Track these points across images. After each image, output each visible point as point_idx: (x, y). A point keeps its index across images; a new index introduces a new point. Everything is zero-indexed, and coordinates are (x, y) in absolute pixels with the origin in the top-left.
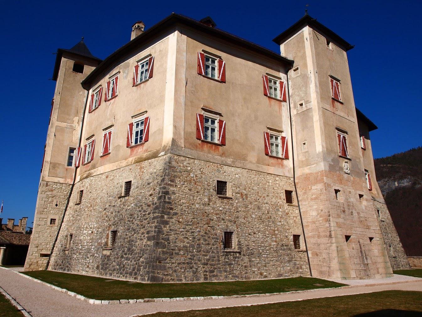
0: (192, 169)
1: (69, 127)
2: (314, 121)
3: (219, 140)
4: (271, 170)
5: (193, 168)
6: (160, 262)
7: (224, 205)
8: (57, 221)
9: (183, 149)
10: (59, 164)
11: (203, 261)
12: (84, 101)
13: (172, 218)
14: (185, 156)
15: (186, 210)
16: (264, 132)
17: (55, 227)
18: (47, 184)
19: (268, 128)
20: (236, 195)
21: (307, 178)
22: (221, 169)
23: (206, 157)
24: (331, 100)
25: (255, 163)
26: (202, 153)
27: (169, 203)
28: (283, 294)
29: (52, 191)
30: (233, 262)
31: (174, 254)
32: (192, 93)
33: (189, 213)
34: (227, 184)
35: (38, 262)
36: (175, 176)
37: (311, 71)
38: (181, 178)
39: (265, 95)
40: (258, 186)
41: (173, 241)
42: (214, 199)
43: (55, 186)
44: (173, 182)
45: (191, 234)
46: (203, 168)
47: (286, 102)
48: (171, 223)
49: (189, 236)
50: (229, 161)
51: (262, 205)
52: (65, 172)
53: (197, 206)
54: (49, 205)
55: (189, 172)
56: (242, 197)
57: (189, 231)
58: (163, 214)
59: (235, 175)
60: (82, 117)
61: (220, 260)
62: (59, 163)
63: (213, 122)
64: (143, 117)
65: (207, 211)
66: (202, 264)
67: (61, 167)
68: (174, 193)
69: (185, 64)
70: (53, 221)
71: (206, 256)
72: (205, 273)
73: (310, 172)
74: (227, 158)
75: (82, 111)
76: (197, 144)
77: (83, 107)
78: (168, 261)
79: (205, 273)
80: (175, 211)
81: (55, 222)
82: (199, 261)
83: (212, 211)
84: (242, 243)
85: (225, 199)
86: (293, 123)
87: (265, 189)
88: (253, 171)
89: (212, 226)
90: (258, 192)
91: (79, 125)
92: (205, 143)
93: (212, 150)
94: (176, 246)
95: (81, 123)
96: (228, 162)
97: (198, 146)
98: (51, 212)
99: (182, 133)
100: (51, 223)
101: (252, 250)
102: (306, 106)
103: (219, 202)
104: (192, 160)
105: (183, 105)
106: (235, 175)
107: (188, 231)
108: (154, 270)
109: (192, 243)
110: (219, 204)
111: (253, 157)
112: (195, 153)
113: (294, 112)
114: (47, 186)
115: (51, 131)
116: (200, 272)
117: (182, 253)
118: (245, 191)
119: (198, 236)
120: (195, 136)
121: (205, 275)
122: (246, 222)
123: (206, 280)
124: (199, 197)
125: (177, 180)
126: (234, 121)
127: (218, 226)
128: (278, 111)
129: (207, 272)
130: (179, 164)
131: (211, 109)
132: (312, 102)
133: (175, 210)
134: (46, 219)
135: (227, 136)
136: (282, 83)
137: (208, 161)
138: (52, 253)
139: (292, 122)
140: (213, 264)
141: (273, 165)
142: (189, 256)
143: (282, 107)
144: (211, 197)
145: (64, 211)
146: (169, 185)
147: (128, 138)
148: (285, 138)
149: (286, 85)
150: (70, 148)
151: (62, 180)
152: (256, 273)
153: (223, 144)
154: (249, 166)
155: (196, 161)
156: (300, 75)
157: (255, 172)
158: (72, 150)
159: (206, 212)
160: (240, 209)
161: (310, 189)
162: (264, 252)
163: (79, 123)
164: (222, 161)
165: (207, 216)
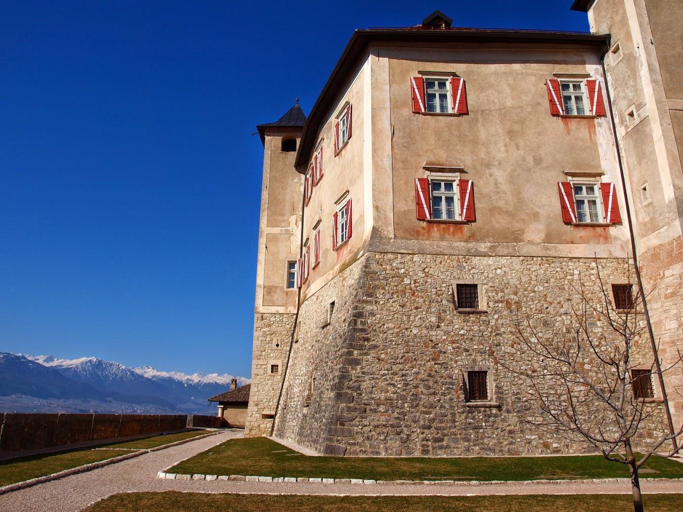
0: (407, 272)
1: (283, 232)
2: (655, 141)
3: (461, 215)
4: (580, 250)
5: (411, 269)
6: (342, 424)
7: (468, 326)
8: (280, 368)
9: (392, 241)
10: (276, 287)
11: (422, 422)
12: (301, 191)
13: (367, 354)
14: (395, 252)
15: (393, 339)
16: (558, 183)
17: (279, 377)
18: (262, 317)
19: (567, 174)
20: (496, 305)
21: (655, 254)
22: (465, 264)
23: (435, 247)
25: (540, 243)
26: (427, 242)
27: (363, 330)
28: (514, 484)
29: (270, 326)
30: (484, 424)
31: (368, 411)
32: (404, 147)
33: (398, 345)
34: (479, 287)
35: (259, 426)
36: (376, 287)
37: (638, 43)
38: (387, 288)
39: (554, 115)
40: (546, 285)
41: (368, 391)
42: (448, 316)
43: (273, 319)
44: (371, 297)
45: (401, 379)
46: (431, 267)
47: (605, 116)
48: (364, 363)
49: (397, 381)
50: (483, 247)
51: (553, 319)
52: (285, 298)
53: (415, 331)
54: (267, 345)
55: (401, 278)
56: (510, 308)
57: (396, 374)
58: (352, 350)
59: (496, 269)
60: (301, 213)
61: (457, 420)
62: (276, 285)
63: (449, 186)
64: (344, 203)
65: (434, 338)
66: (420, 428)
67: (278, 291)
68: (372, 314)
69: (388, 105)
70: (274, 368)
71: (430, 413)
72: (424, 443)
73: (660, 243)
74: (478, 244)
75: (300, 206)
76: (419, 229)
77: (300, 200)
78: (356, 422)
79: (424, 443)
80: (373, 343)
81: (277, 369)
82: (415, 422)
83: (444, 337)
84: (506, 390)
85: (471, 315)
86: (623, 154)
87: (562, 288)
88: (535, 259)
89: (443, 363)
90: (546, 295)
91: (297, 227)
92: (435, 225)
93: (449, 235)
94: (372, 399)
95: (300, 223)
96: (479, 249)
97: (422, 231)
98: (272, 355)
99: (391, 215)
100: (272, 372)
101: (526, 401)
102: (639, 115)
103: (458, 322)
104: (408, 257)
105: (389, 170)
106: (494, 271)
107: (395, 374)
108: (332, 437)
109: (402, 393)
110: (458, 324)
111: (535, 233)
112: (414, 243)
113: (621, 132)
114: (262, 320)
115: (262, 241)
116: (414, 440)
117: (382, 408)
118: (515, 297)
119: (415, 380)
120: (414, 217)
121: (423, 446)
122: (515, 352)
123: (425, 454)
124: (419, 316)
125: (379, 293)
126: (491, 175)
127: (456, 362)
128: (588, 136)
129: (427, 440)
130: (384, 267)
131: (442, 165)
132: (648, 105)
133: (374, 340)
134: (265, 366)
135: (478, 205)
136: (591, 85)
137: (439, 253)
138: (276, 414)
139: (620, 151)
140: (441, 427)
142: (396, 415)
143: (596, 127)
144: (443, 315)
145: (288, 353)
146: (367, 302)
147: (333, 236)
148: (609, 184)
149: (603, 85)
150: (288, 261)
151: (281, 310)
152: (534, 443)
153: (471, 218)
154: (526, 249)
155: (416, 258)
156: (623, 58)
157: (540, 258)
158: (292, 265)
159: (432, 341)
160: (502, 330)
161: (662, 277)
162: (554, 404)
163: (297, 223)
164: (469, 250)
165: (434, 347)
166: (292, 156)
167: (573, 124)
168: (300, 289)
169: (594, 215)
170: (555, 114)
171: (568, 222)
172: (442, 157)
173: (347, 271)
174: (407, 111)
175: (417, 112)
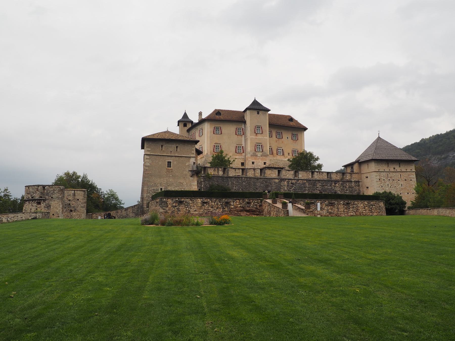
39: (236, 134)
47: (244, 135)
64: (201, 146)
69: (209, 132)
136: (243, 129)
141: (238, 155)
149: (244, 130)
166: (186, 128)
167: (239, 136)
169: (240, 151)
170: (236, 134)
173: (202, 159)
175: (214, 133)
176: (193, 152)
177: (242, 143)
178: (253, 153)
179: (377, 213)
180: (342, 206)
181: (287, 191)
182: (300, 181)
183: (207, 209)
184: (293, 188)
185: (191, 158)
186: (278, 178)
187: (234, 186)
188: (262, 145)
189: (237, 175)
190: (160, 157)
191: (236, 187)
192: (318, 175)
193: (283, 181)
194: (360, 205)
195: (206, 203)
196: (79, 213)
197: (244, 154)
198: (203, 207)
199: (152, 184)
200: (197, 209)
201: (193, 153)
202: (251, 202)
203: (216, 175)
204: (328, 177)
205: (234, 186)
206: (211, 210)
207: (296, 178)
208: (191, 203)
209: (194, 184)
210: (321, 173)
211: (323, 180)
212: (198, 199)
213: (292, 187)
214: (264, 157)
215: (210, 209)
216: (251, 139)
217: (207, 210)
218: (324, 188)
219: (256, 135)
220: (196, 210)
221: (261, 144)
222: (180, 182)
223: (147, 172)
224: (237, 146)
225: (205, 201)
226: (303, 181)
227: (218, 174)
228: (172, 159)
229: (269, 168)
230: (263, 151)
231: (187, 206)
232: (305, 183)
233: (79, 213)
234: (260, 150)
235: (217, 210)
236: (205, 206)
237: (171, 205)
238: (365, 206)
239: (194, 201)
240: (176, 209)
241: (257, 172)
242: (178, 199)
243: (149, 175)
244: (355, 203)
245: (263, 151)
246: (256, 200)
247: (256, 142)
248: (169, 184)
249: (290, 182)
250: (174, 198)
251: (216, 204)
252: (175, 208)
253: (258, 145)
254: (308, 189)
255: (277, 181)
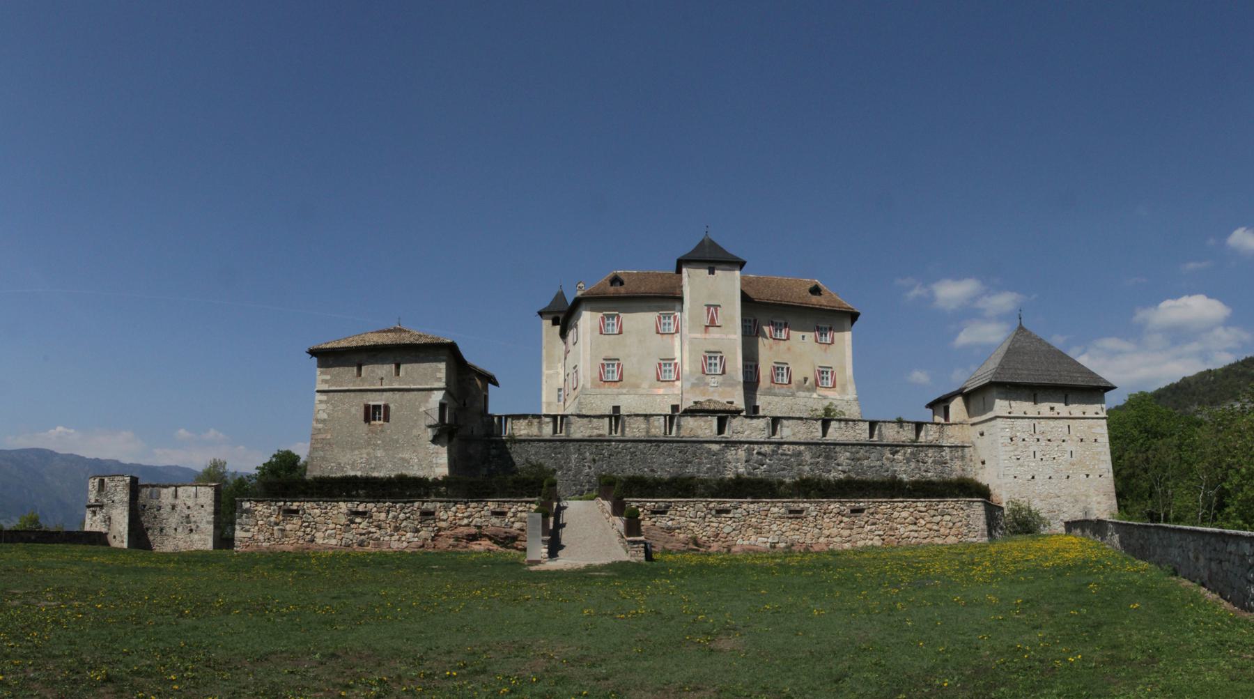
4: (661, 391)
24: (704, 327)
36: (583, 408)
50: (624, 391)
55: (592, 404)
99: (589, 379)
112: (598, 391)
120: (598, 379)
141: (664, 387)
153: (621, 380)
154: (641, 391)
155: (598, 396)
166: (558, 328)
168: (564, 403)
170: (658, 333)
171: (658, 380)
172: (611, 355)
174: (598, 332)
176: (439, 375)
177: (674, 355)
178: (698, 379)
179: (960, 536)
180: (834, 519)
181: (746, 475)
182: (785, 446)
183: (364, 531)
184: (765, 466)
185: (435, 392)
186: (717, 439)
187: (586, 464)
188: (721, 358)
189: (594, 434)
190: (353, 394)
191: (590, 468)
192: (840, 428)
193: (733, 449)
194: (899, 514)
195: (363, 514)
196: (203, 536)
197: (678, 383)
198: (352, 526)
199: (332, 464)
200: (334, 531)
201: (440, 378)
202: (507, 510)
203: (535, 436)
204: (871, 435)
205: (586, 464)
206: (376, 535)
207: (776, 438)
208: (318, 515)
209: (439, 461)
210: (851, 423)
211: (858, 445)
212: (338, 502)
213: (762, 465)
214: (729, 389)
215: (373, 533)
216: (692, 342)
217: (364, 534)
218: (861, 464)
219: (704, 331)
220: (332, 534)
221: (719, 355)
222: (402, 459)
223: (320, 437)
224: (662, 362)
225: (361, 508)
226: (797, 447)
227: (539, 434)
228: (383, 397)
229: (691, 412)
230: (724, 372)
231: (307, 524)
232: (800, 453)
233: (203, 536)
234: (715, 370)
235: (396, 534)
236: (360, 523)
237: (265, 519)
238: (915, 516)
239: (326, 508)
240: (279, 529)
241: (656, 424)
242: (282, 503)
243: (325, 442)
244: (882, 507)
245: (724, 372)
246: (524, 504)
247: (705, 349)
248: (373, 466)
249: (755, 452)
250: (273, 501)
251: (393, 518)
252: (276, 528)
253: (710, 358)
254: (811, 469)
255: (715, 447)
